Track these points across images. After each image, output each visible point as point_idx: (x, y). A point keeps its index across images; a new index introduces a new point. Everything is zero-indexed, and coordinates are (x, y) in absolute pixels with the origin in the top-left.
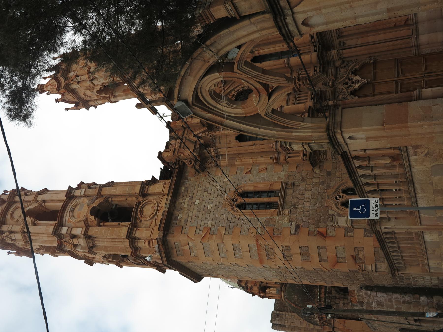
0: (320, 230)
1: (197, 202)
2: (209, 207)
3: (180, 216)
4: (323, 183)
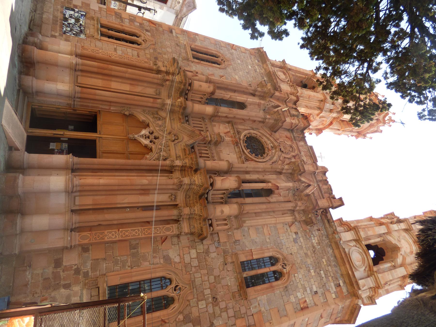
1: (250, 67)
2: (239, 61)
3: (257, 61)
4: (159, 53)
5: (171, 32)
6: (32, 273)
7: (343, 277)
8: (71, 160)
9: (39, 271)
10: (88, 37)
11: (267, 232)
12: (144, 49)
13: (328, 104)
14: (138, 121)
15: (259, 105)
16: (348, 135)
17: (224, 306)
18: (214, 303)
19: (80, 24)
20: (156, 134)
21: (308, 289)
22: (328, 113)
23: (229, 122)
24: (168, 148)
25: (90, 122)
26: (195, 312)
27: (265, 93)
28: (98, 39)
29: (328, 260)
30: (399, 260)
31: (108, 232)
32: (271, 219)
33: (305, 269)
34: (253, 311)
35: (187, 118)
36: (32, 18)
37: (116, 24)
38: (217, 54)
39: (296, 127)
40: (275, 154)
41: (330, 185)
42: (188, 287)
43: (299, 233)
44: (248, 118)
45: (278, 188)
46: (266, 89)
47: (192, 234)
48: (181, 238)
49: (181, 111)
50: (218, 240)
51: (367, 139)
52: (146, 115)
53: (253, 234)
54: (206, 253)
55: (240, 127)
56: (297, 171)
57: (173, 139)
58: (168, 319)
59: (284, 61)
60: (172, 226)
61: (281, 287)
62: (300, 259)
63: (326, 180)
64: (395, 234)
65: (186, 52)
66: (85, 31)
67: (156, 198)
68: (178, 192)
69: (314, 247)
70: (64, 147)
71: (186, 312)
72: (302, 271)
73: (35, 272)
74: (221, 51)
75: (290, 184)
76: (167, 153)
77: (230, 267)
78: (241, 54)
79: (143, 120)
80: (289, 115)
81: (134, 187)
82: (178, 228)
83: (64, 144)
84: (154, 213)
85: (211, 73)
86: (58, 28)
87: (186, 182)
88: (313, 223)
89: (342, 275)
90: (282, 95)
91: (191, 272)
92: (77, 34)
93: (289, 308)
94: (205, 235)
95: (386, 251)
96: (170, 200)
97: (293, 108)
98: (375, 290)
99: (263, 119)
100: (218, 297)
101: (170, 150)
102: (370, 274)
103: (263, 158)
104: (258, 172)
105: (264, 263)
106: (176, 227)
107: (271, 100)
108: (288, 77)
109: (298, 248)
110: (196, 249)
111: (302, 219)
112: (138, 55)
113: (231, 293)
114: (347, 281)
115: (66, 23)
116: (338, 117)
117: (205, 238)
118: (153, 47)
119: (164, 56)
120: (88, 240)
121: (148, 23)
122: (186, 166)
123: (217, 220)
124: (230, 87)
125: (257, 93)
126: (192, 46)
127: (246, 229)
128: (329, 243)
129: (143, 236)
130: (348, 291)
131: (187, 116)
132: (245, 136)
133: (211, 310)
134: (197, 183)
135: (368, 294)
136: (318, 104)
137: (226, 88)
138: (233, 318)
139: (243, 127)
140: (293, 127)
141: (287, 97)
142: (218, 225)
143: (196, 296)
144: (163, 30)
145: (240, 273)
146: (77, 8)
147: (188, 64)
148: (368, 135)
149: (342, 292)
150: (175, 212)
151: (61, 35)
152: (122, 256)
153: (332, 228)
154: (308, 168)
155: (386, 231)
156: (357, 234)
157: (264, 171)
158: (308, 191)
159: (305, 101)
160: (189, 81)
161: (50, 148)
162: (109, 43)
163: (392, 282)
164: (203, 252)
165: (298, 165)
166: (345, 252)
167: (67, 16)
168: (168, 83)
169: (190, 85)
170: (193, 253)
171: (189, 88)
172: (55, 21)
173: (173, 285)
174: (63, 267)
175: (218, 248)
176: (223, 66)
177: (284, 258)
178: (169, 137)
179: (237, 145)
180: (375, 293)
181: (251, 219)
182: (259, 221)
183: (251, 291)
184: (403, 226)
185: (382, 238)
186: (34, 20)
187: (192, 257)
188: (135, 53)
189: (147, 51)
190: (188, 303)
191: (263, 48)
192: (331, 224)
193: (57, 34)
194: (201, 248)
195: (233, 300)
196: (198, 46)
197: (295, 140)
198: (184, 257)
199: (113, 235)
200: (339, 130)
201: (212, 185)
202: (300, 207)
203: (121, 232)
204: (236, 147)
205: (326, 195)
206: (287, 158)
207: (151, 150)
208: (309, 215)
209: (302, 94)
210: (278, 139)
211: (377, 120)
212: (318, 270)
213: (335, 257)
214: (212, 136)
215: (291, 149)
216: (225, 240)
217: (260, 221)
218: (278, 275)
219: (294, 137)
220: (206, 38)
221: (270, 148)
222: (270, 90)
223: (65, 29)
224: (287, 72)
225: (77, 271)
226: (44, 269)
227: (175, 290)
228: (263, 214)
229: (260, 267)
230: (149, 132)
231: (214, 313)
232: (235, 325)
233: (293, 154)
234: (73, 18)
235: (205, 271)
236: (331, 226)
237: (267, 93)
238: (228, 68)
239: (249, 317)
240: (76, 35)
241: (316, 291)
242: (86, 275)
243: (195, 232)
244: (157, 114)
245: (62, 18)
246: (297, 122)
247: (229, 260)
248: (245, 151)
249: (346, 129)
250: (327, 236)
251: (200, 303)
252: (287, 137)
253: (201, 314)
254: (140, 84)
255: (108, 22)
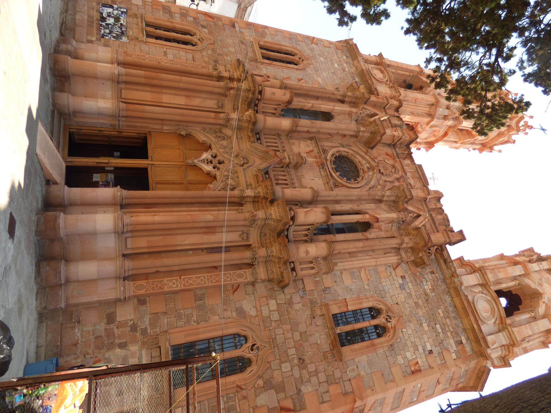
0: (212, 20)
1: (336, 66)
2: (322, 59)
3: (345, 57)
4: (219, 55)
5: (234, 26)
6: (82, 331)
7: (466, 332)
8: (119, 193)
9: (89, 328)
10: (132, 40)
11: (366, 276)
12: (201, 51)
13: (441, 109)
14: (197, 142)
15: (350, 114)
16: (468, 148)
17: (313, 369)
18: (301, 366)
19: (121, 24)
20: (219, 158)
21: (420, 348)
22: (441, 121)
23: (311, 139)
24: (236, 174)
25: (138, 147)
26: (277, 377)
27: (357, 98)
28: (143, 41)
29: (446, 311)
30: (541, 310)
31: (167, 280)
32: (370, 261)
33: (416, 322)
34: (350, 375)
35: (258, 136)
36: (63, 20)
37: (165, 21)
38: (293, 52)
39: (399, 141)
40: (372, 177)
41: (446, 215)
42: (267, 346)
43: (407, 277)
44: (336, 132)
45: (377, 220)
46: (358, 93)
47: (270, 280)
48: (257, 286)
49: (251, 126)
50: (303, 288)
51: (495, 153)
52: (207, 134)
53: (347, 280)
54: (288, 304)
55: (326, 144)
56: (402, 198)
57: (242, 163)
58: (245, 384)
59: (380, 55)
60: (245, 272)
61: (384, 345)
62: (409, 309)
63: (441, 208)
64: (536, 276)
65: (254, 51)
66: (127, 32)
67: (224, 238)
68: (251, 229)
69: (426, 294)
70: (110, 178)
71: (266, 376)
72: (412, 325)
73: (85, 329)
74: (299, 47)
75: (394, 215)
76: (235, 181)
77: (319, 321)
78: (324, 49)
79: (203, 141)
80: (389, 125)
81: (196, 225)
82: (253, 274)
83: (109, 174)
84: (223, 256)
85: (286, 76)
86: (95, 31)
87: (261, 217)
88: (424, 263)
89: (464, 329)
90: (380, 100)
91: (271, 328)
92: (117, 37)
93: (396, 371)
94: (287, 281)
95: (522, 298)
96: (241, 239)
97: (394, 116)
98: (508, 348)
99: (356, 132)
100: (305, 358)
101: (238, 177)
102: (502, 327)
103: (358, 183)
104: (351, 201)
105: (362, 315)
106: (250, 273)
107: (366, 107)
108: (387, 76)
109: (406, 295)
110: (276, 299)
111: (410, 260)
112: (193, 59)
113: (322, 354)
114: (472, 337)
115: (104, 24)
116: (455, 126)
117: (287, 285)
118: (212, 47)
119: (225, 57)
120: (144, 290)
121: (204, 17)
122: (259, 196)
123: (300, 263)
124: (311, 93)
125: (346, 99)
126: (261, 43)
127: (338, 273)
128: (447, 290)
129: (210, 284)
130: (472, 350)
131: (258, 134)
132: (333, 155)
133: (297, 374)
134: (274, 217)
135: (500, 353)
136: (428, 109)
137: (307, 95)
138: (326, 384)
139: (330, 144)
140: (395, 141)
141: (386, 102)
142: (302, 269)
143: (278, 357)
144: (224, 24)
145: (332, 328)
146: (115, 4)
147: (257, 67)
148: (496, 148)
149: (465, 351)
150: (247, 255)
151: (98, 39)
152: (185, 309)
153: (451, 269)
154: (417, 193)
155: (523, 272)
156: (484, 276)
157: (359, 200)
158: (418, 223)
159: (410, 107)
160: (259, 88)
161: (94, 180)
162: (157, 45)
163: (532, 338)
164: (285, 303)
165: (404, 190)
166: (468, 301)
167: (104, 15)
168: (232, 92)
169: (260, 93)
170: (273, 304)
171: (260, 97)
172: (90, 22)
173: (249, 344)
174: (116, 323)
175: (303, 297)
176: (301, 66)
177: (389, 309)
178: (236, 161)
179: (323, 168)
180: (509, 352)
181: (344, 260)
182: (355, 262)
183: (347, 350)
184: (545, 265)
185: (518, 282)
186: (65, 23)
187: (271, 309)
188: (190, 56)
189: (204, 53)
190: (268, 365)
191: (352, 39)
192: (448, 264)
193: (94, 39)
194: (281, 298)
195: (324, 361)
196: (268, 42)
197: (399, 158)
198: (261, 310)
199: (174, 284)
200: (456, 142)
201: (293, 219)
202: (407, 243)
203: (184, 279)
204: (322, 170)
205: (442, 228)
206: (389, 181)
207: (215, 178)
208: (419, 253)
209: (406, 97)
210: (376, 158)
211: (509, 126)
212: (432, 323)
213: (455, 306)
214: (291, 157)
215: (393, 170)
216: (312, 288)
217: (355, 263)
218: (380, 331)
219: (397, 153)
220: (277, 31)
221: (366, 169)
222: (363, 93)
223: (103, 32)
224: (385, 69)
225: (134, 328)
226: (95, 325)
227: (252, 350)
228: (360, 255)
229: (357, 321)
230: (212, 156)
231: (301, 377)
232: (328, 392)
233: (397, 176)
234: (112, 17)
235: (289, 327)
236: (448, 268)
237: (360, 98)
238: (307, 69)
239: (345, 383)
240: (117, 38)
241: (431, 351)
242: (144, 332)
243: (273, 278)
244: (221, 132)
245: (99, 18)
246: (401, 134)
247: (318, 312)
248: (334, 175)
249: (465, 141)
250: (444, 280)
251: (283, 365)
252: (387, 155)
253: (285, 379)
254: (197, 95)
255: (155, 19)
